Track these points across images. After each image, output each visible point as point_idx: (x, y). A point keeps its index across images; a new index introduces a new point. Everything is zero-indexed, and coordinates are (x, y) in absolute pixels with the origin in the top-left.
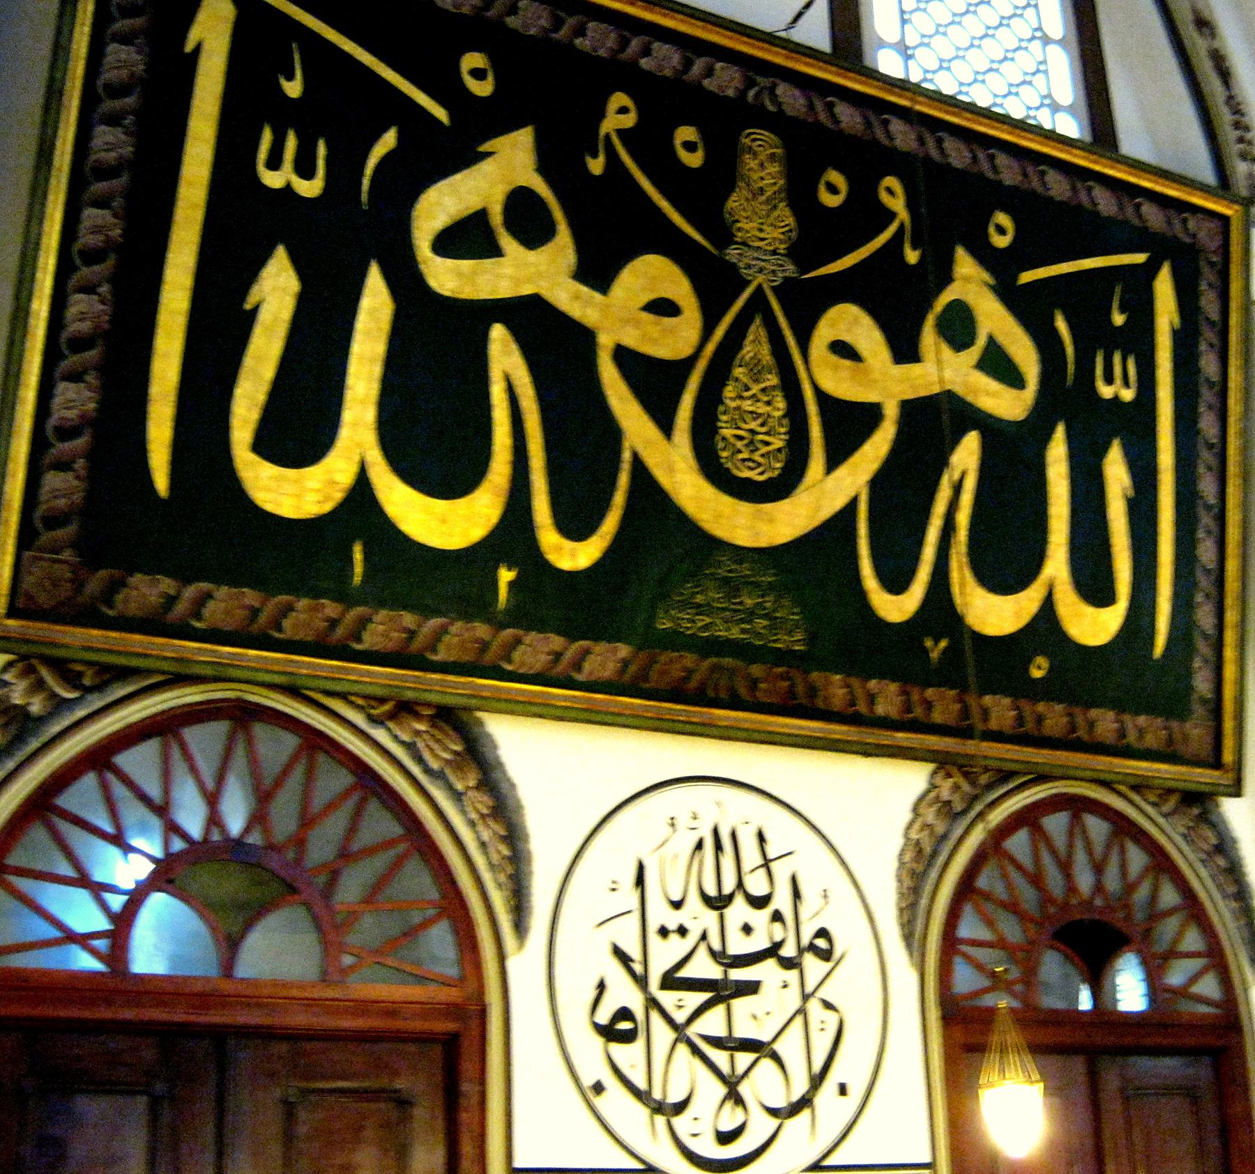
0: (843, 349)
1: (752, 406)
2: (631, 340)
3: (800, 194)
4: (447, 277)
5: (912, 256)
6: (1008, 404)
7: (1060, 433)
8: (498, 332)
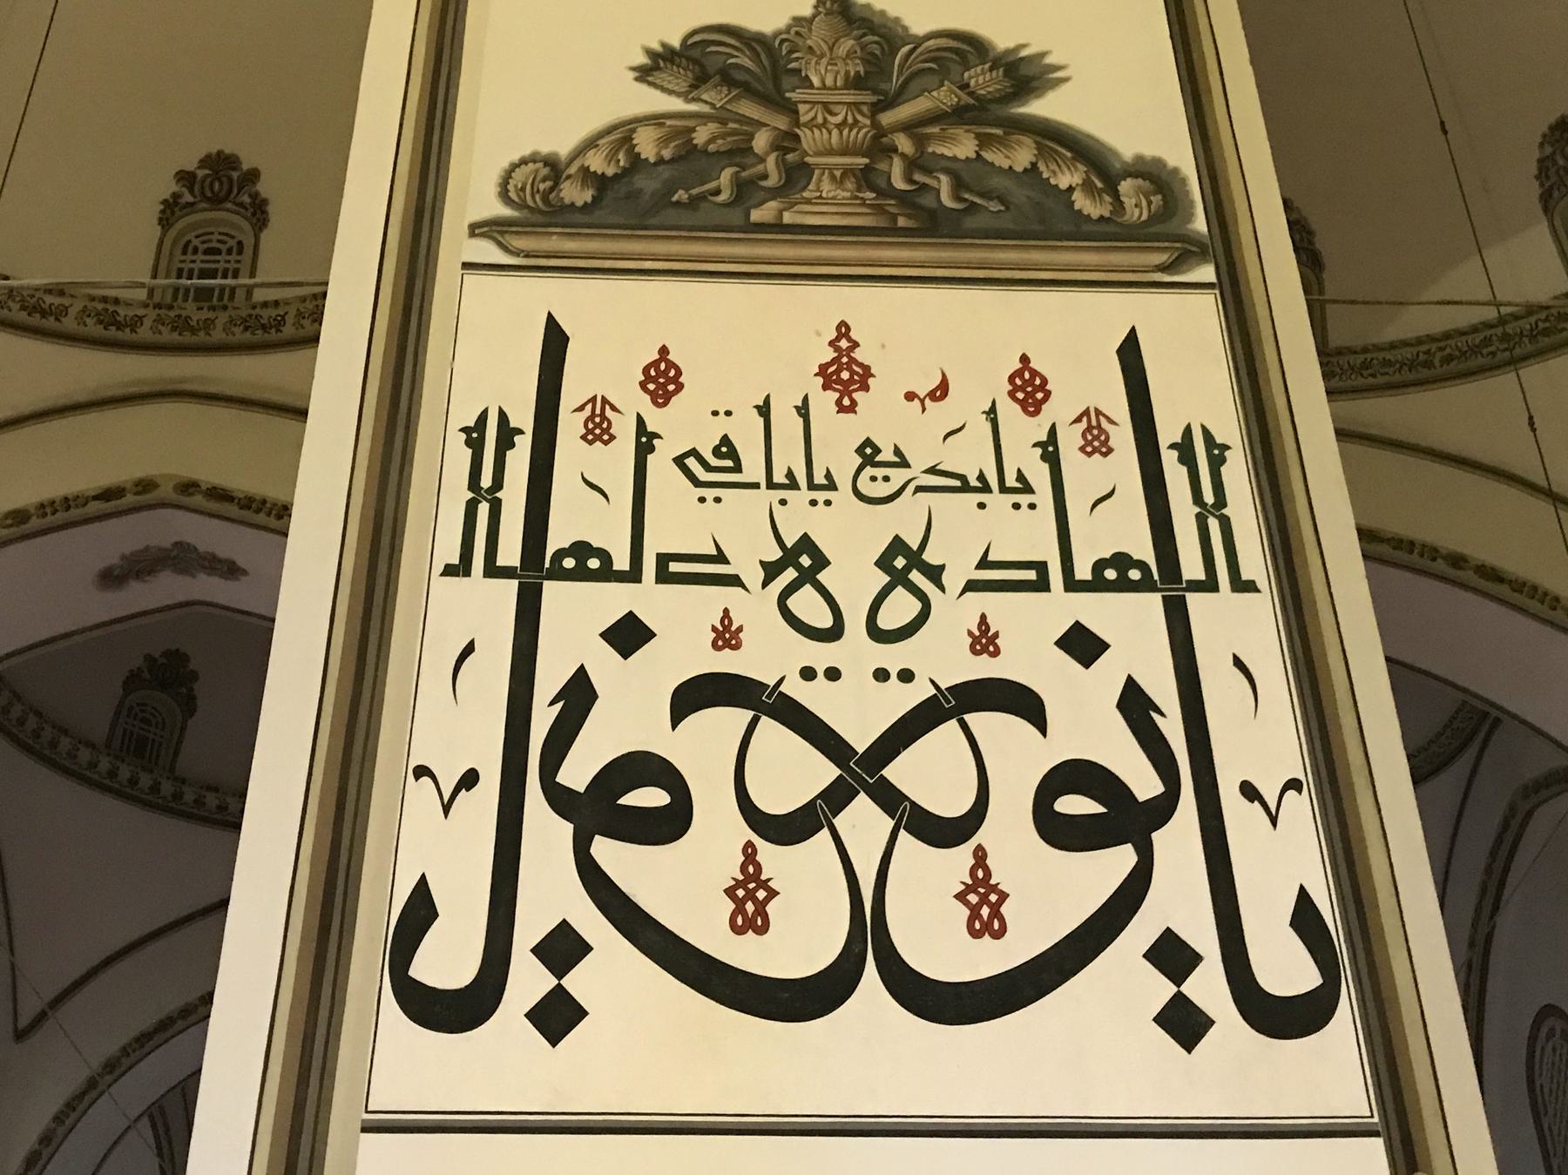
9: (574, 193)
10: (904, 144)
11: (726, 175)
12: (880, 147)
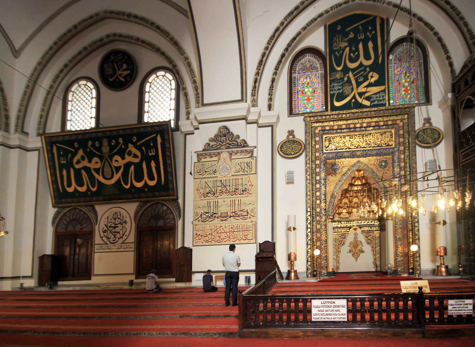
0: (116, 161)
1: (107, 170)
2: (95, 167)
3: (110, 145)
4: (77, 167)
5: (123, 147)
6: (137, 160)
7: (144, 162)
8: (82, 171)
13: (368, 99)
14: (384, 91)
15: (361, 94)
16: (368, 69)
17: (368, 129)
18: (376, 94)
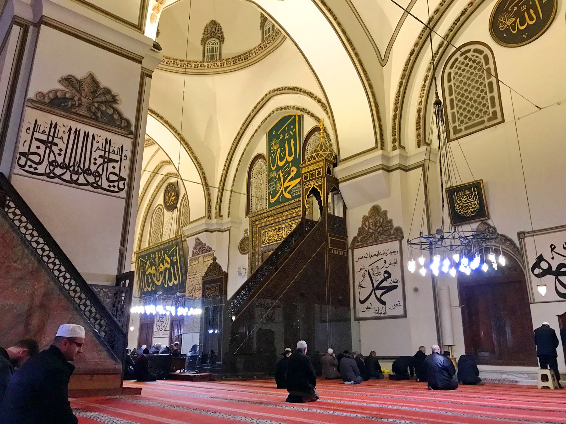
6: (168, 266)
9: (47, 100)
10: (96, 105)
11: (70, 104)
12: (92, 104)
13: (289, 192)
14: (299, 183)
15: (286, 188)
16: (290, 165)
17: (288, 221)
18: (295, 186)
